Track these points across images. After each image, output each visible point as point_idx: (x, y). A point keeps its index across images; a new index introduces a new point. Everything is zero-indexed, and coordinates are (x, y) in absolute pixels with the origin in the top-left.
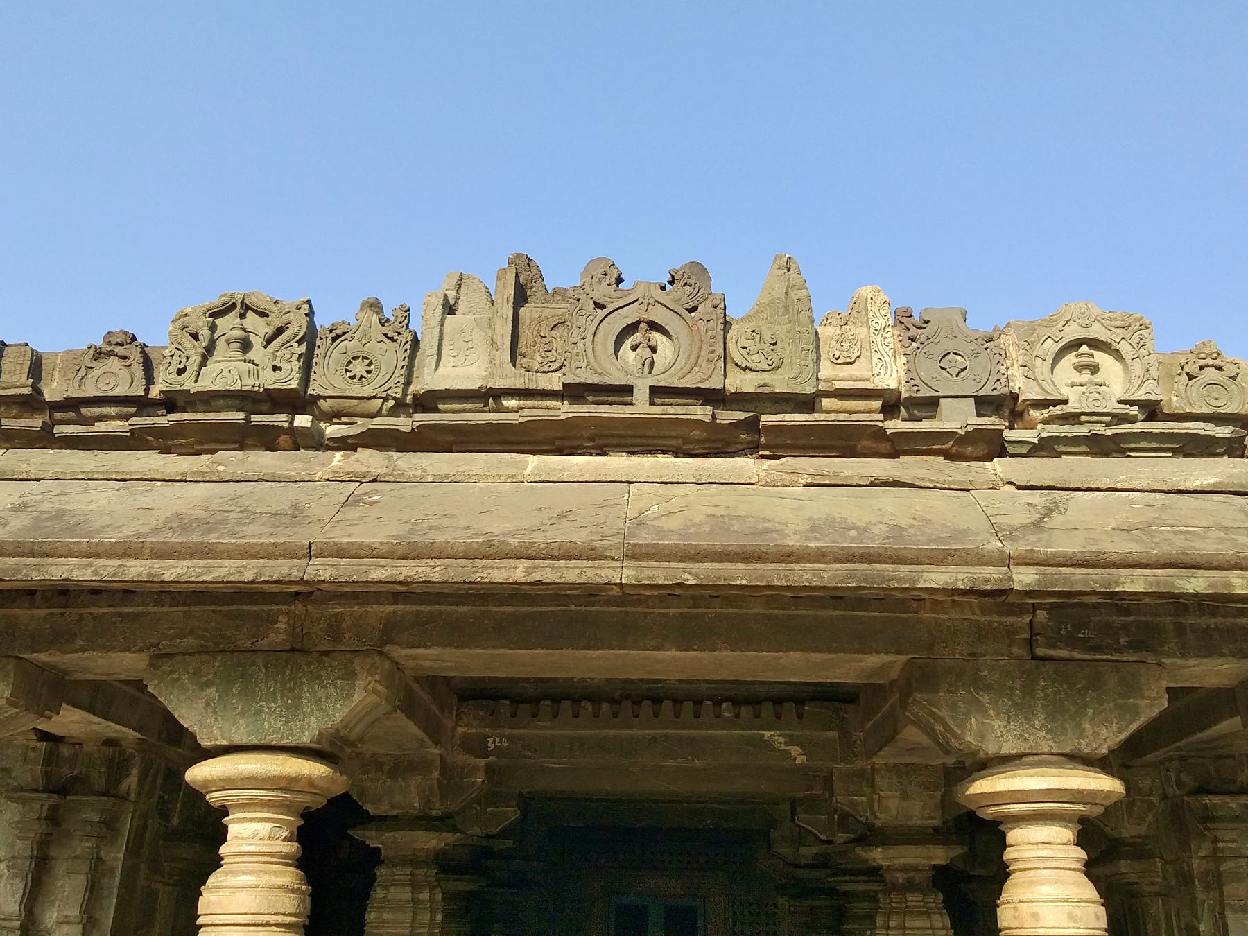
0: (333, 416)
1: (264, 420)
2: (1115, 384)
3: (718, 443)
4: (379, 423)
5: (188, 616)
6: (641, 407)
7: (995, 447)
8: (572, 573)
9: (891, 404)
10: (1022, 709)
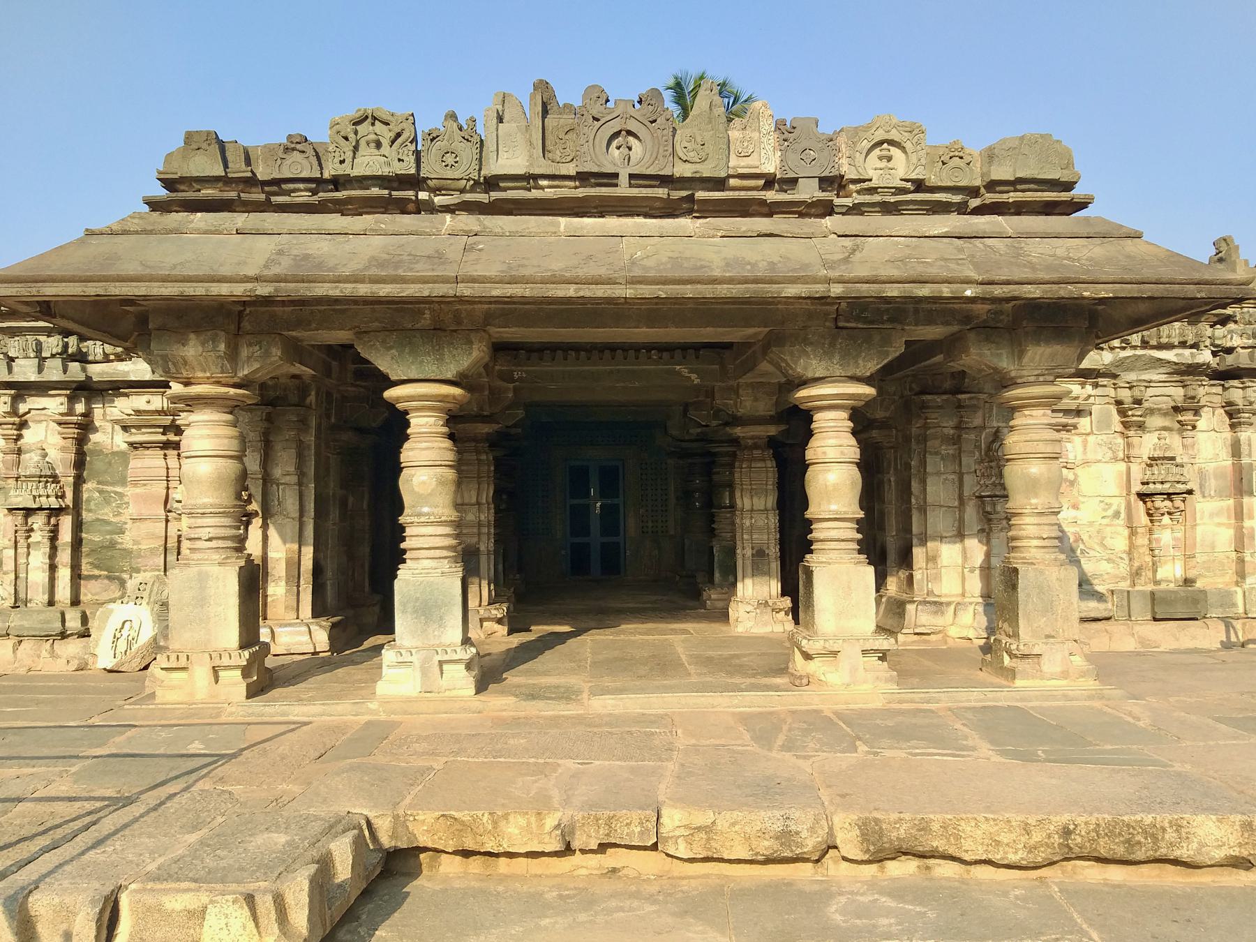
0: (436, 191)
1: (400, 194)
2: (901, 168)
3: (669, 210)
4: (468, 197)
5: (374, 311)
6: (624, 189)
7: (827, 209)
8: (600, 291)
9: (770, 182)
10: (828, 354)
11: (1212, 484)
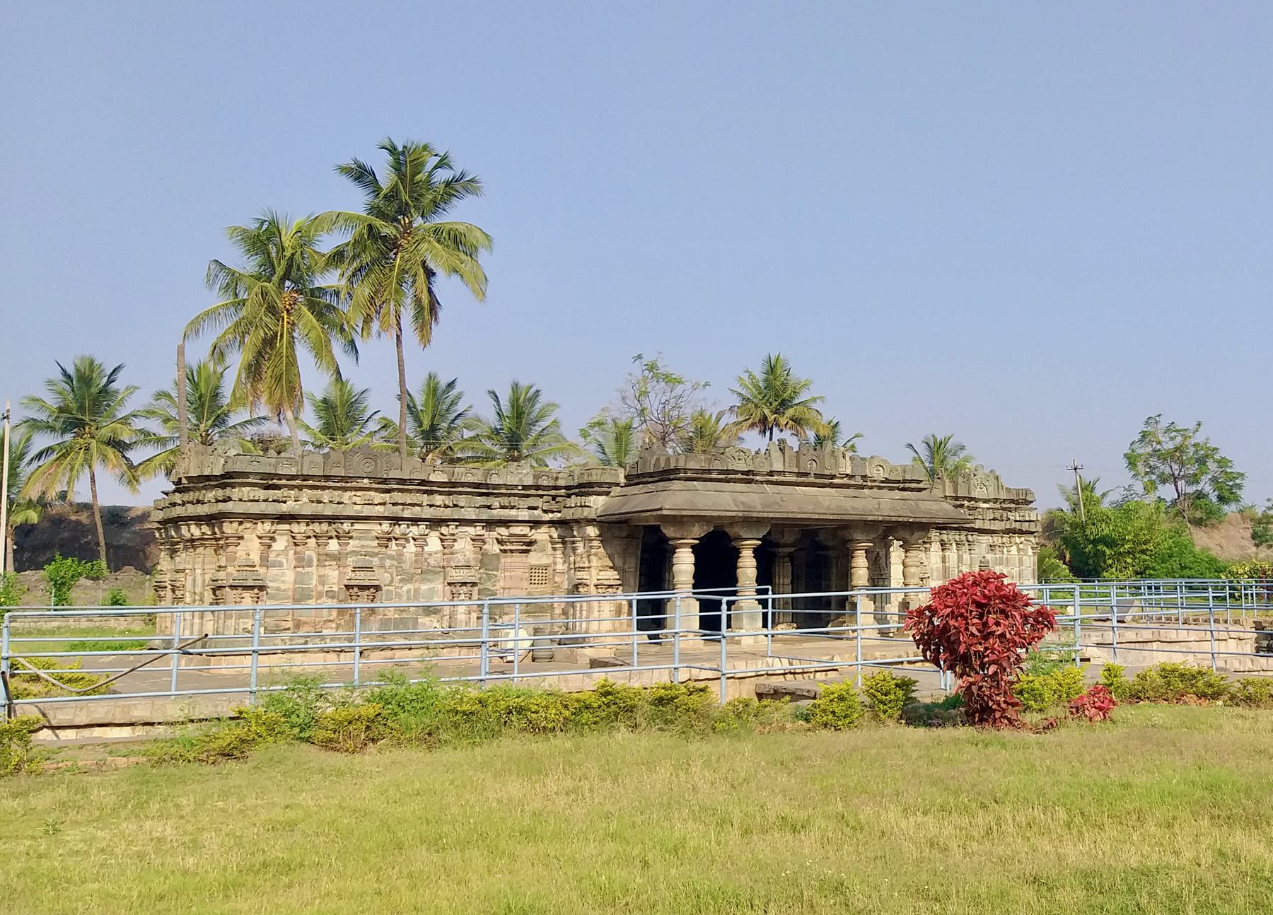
6: (812, 479)
7: (863, 487)
11: (935, 574)
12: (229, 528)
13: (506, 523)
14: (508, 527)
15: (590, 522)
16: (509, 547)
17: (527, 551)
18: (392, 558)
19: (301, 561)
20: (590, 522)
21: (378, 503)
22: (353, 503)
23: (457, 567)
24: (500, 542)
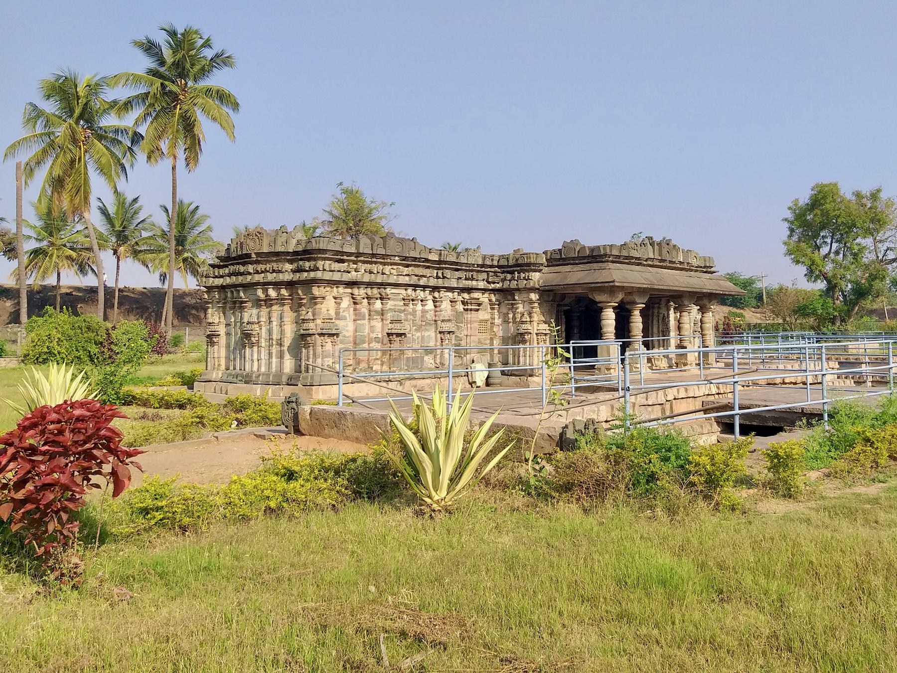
12: (316, 291)
13: (469, 290)
14: (469, 293)
15: (533, 290)
16: (469, 307)
17: (477, 310)
18: (410, 314)
19: (358, 316)
20: (533, 290)
21: (404, 274)
22: (392, 273)
23: (443, 321)
24: (463, 303)
